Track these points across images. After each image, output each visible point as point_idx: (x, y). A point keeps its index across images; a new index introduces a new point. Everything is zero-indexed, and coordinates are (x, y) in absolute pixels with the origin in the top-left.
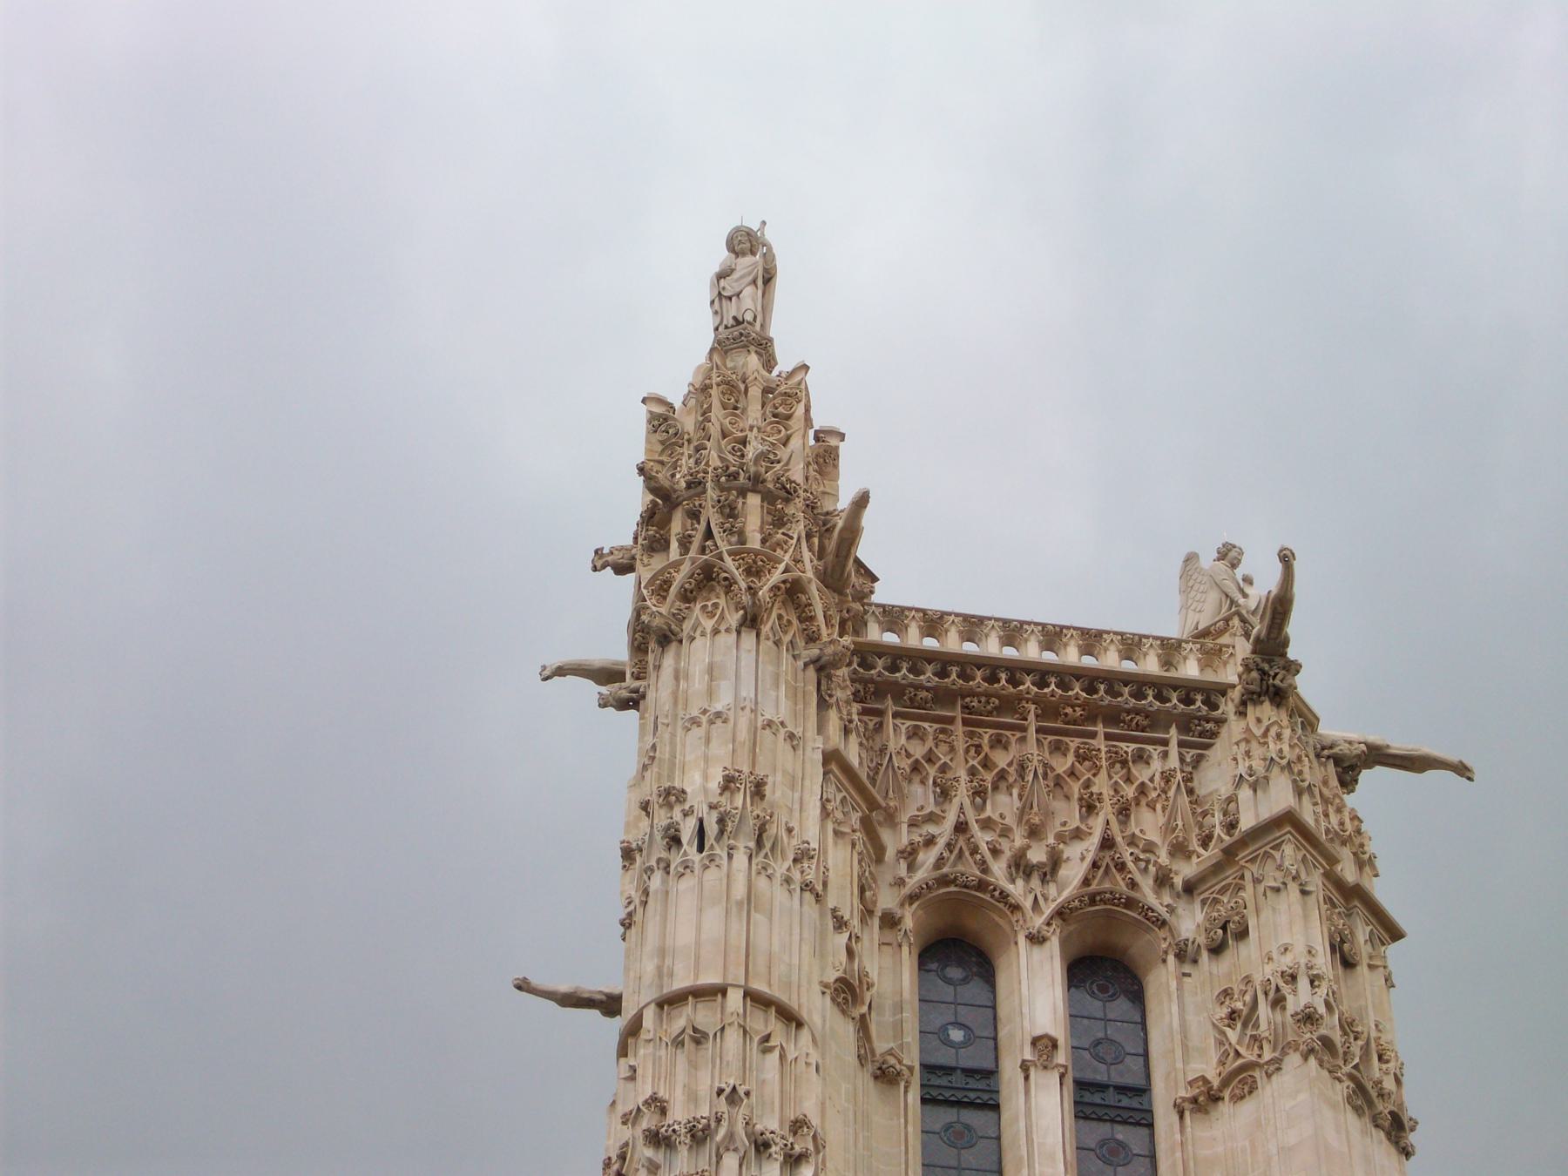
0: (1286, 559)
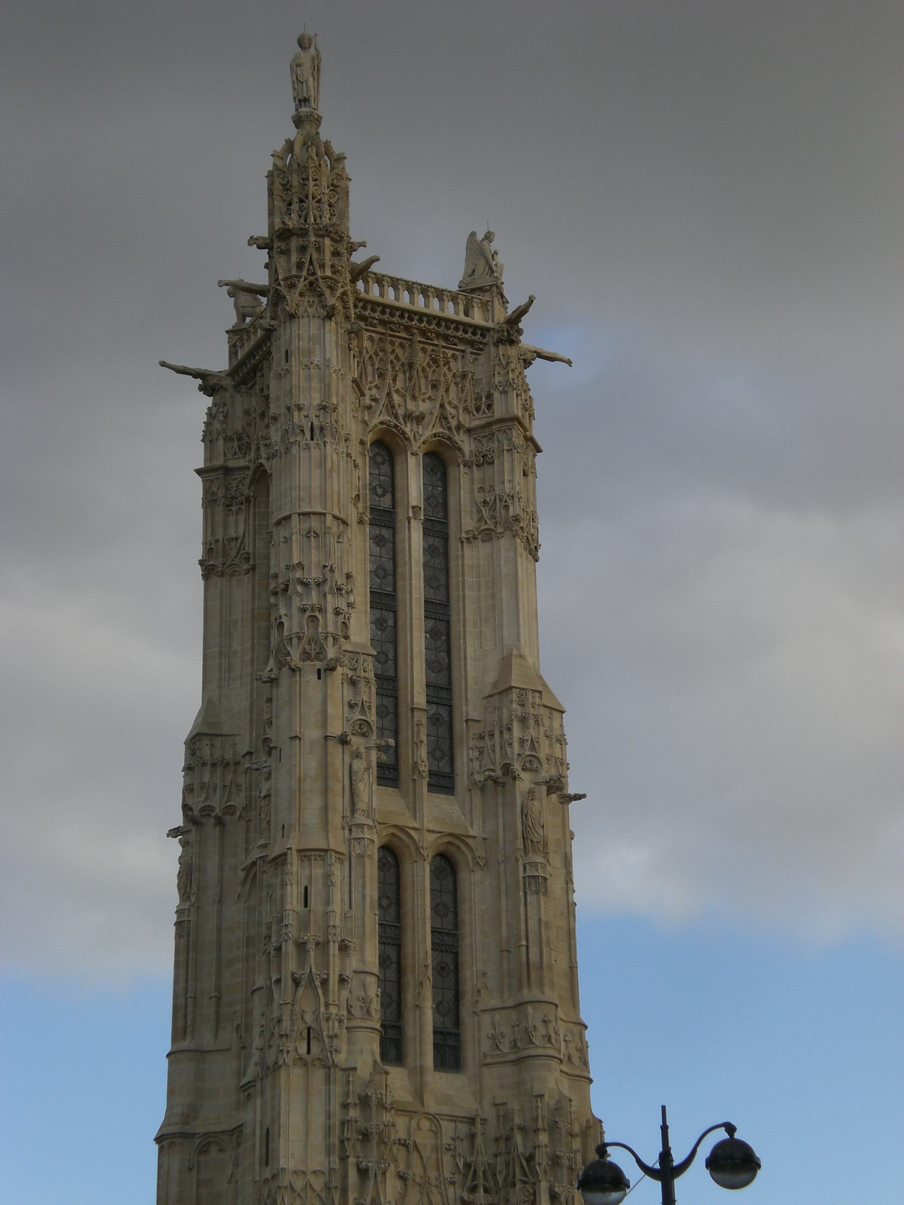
0: (531, 301)
